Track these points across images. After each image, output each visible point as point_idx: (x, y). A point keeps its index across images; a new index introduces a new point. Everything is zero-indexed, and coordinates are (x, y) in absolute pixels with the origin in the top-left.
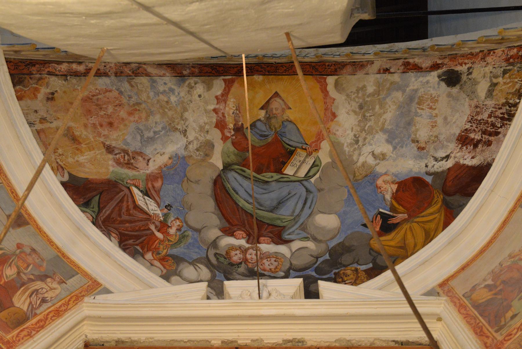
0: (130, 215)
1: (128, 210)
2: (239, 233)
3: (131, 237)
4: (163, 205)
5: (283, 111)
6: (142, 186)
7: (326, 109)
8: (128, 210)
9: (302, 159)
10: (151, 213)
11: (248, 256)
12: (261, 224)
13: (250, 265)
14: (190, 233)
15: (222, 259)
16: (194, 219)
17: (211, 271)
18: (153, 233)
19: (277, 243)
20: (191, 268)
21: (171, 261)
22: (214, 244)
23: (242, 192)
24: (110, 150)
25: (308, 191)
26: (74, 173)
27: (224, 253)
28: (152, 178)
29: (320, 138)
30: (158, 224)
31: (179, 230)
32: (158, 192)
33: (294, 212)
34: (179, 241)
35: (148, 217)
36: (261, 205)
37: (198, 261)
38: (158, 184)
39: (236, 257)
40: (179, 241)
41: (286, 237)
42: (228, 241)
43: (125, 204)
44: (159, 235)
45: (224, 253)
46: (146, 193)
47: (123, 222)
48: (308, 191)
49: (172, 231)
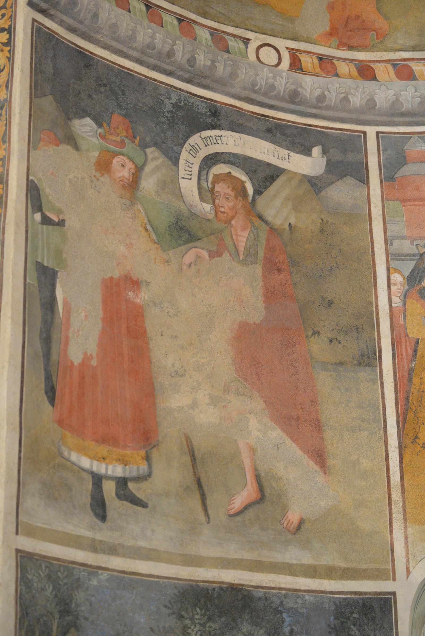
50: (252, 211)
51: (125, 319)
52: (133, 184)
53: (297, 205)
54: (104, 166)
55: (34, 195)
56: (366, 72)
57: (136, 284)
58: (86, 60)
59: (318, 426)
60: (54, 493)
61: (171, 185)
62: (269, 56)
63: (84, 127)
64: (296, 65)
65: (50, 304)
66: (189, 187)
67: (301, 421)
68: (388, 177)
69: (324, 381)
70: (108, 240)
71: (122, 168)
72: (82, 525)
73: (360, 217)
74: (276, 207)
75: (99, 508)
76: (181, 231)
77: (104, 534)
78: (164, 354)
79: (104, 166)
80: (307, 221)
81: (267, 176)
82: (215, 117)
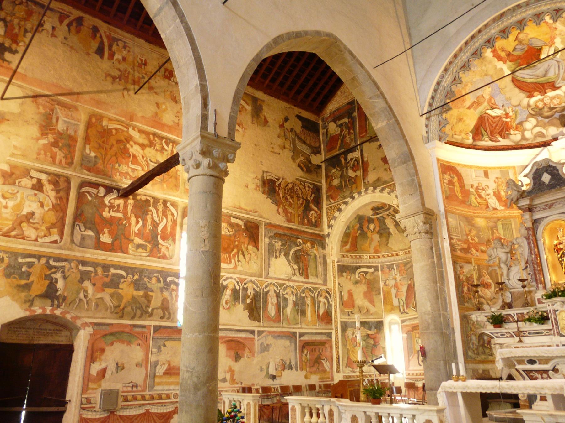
0: (494, 123)
1: (493, 121)
2: (536, 94)
3: (501, 131)
4: (501, 107)
5: (526, 36)
6: (489, 108)
7: (550, 28)
8: (493, 121)
9: (548, 49)
10: (499, 114)
11: (545, 102)
12: (543, 85)
13: (548, 106)
14: (517, 108)
15: (536, 110)
16: (515, 102)
17: (535, 118)
18: (506, 122)
19: (555, 90)
20: (527, 123)
21: (519, 126)
22: (529, 105)
23: (526, 76)
24: (469, 108)
25: (558, 62)
26: (470, 129)
27: (535, 107)
28: (489, 101)
29: (552, 39)
30: (505, 116)
31: (513, 111)
32: (495, 104)
33: (555, 73)
34: (516, 115)
35: (500, 117)
36: (538, 76)
37: (528, 117)
38: (493, 102)
39: (541, 105)
40: (516, 115)
41: (557, 85)
42: (533, 100)
43: (490, 121)
44: (508, 120)
45: (535, 107)
46: (492, 108)
47: (495, 128)
48: (558, 62)
49: (511, 114)
50: (365, 278)
51: (350, 294)
52: (350, 279)
53: (371, 276)
54: (347, 278)
55: (339, 284)
56: (379, 257)
57: (351, 290)
58: (344, 266)
59: (374, 302)
60: (344, 314)
61: (355, 277)
62: (366, 257)
63: (344, 274)
64: (370, 258)
65: (342, 295)
66: (357, 277)
67: (372, 302)
68: (382, 271)
69: (374, 297)
70: (348, 285)
71: (349, 277)
72: (347, 317)
73: (378, 276)
74: (368, 277)
75: (349, 315)
76: (357, 282)
77: (350, 317)
78: (355, 297)
79: (347, 278)
80: (372, 278)
81: (366, 273)
82: (360, 267)
